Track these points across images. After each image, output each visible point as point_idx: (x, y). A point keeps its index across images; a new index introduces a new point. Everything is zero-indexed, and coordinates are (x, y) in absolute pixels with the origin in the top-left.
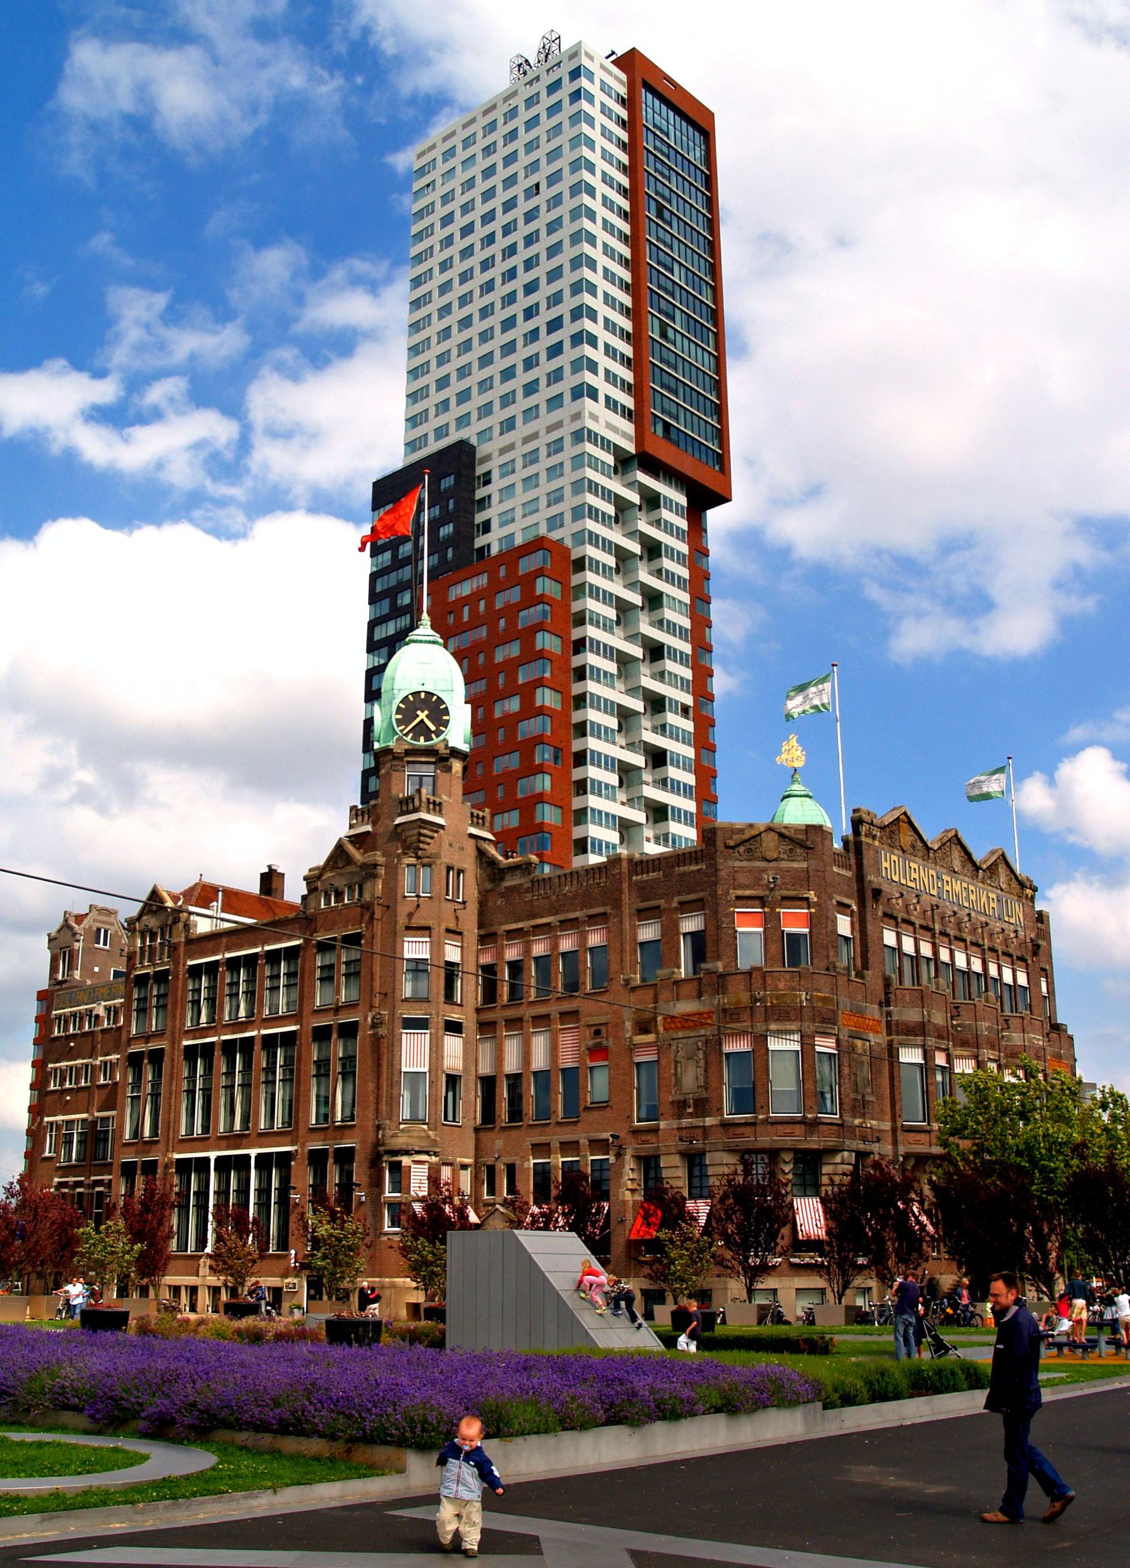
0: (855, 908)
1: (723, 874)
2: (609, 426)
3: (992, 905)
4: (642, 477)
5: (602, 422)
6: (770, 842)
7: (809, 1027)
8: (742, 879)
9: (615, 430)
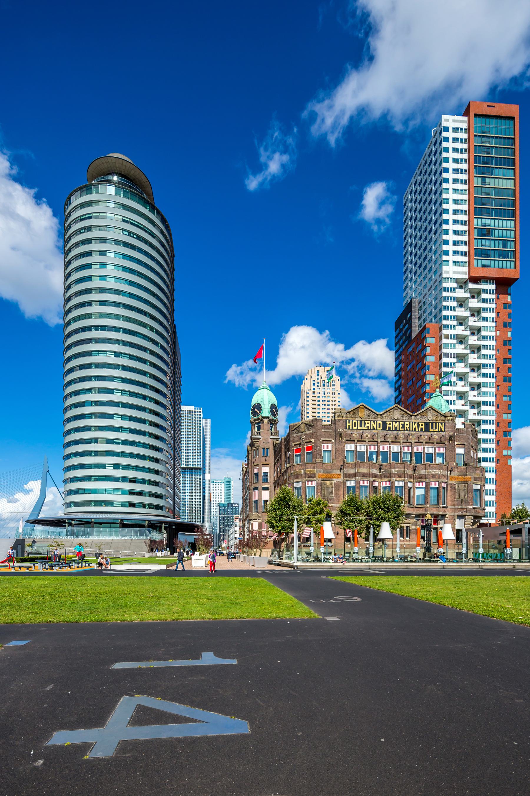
0: (333, 441)
1: (291, 439)
2: (454, 273)
3: (420, 427)
4: (471, 286)
6: (303, 427)
7: (303, 480)
8: (296, 439)
9: (458, 273)
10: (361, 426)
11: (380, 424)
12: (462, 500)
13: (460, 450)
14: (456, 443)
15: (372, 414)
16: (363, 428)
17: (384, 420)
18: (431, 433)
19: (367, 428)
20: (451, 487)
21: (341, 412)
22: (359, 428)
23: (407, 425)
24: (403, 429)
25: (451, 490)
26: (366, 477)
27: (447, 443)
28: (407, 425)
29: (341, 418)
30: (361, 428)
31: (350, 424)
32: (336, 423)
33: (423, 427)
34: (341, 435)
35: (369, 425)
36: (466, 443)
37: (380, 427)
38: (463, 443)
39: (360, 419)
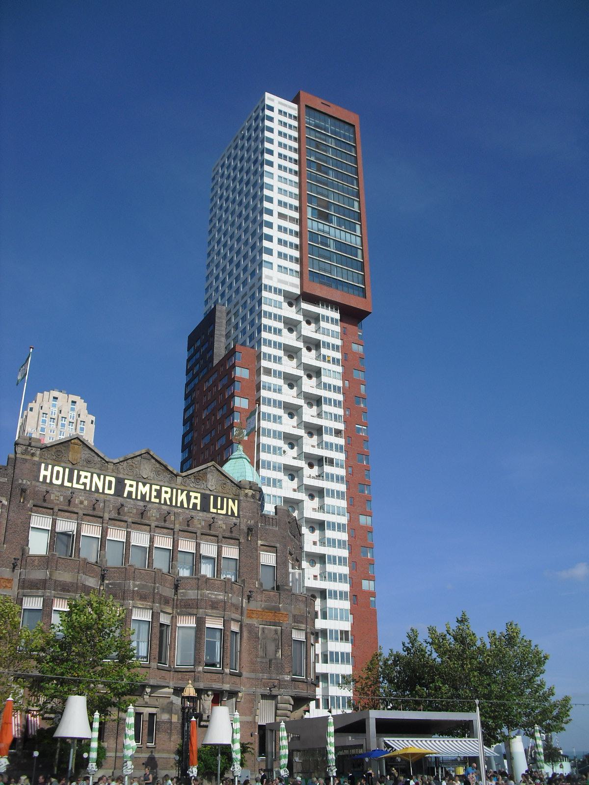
2: (280, 281)
3: (193, 501)
4: (305, 306)
5: (275, 279)
9: (285, 283)
10: (70, 480)
11: (110, 482)
12: (270, 661)
13: (268, 558)
14: (260, 542)
15: (97, 459)
16: (75, 486)
17: (121, 476)
18: (214, 515)
19: (82, 487)
20: (250, 632)
21: (30, 445)
22: (67, 484)
23: (166, 492)
24: (157, 501)
25: (249, 639)
26: (69, 591)
27: (242, 540)
28: (166, 492)
29: (28, 457)
30: (69, 485)
31: (48, 473)
32: (18, 465)
33: (198, 501)
34: (23, 491)
35: (88, 481)
36: (278, 545)
37: (110, 488)
38: (272, 544)
39: (70, 466)
